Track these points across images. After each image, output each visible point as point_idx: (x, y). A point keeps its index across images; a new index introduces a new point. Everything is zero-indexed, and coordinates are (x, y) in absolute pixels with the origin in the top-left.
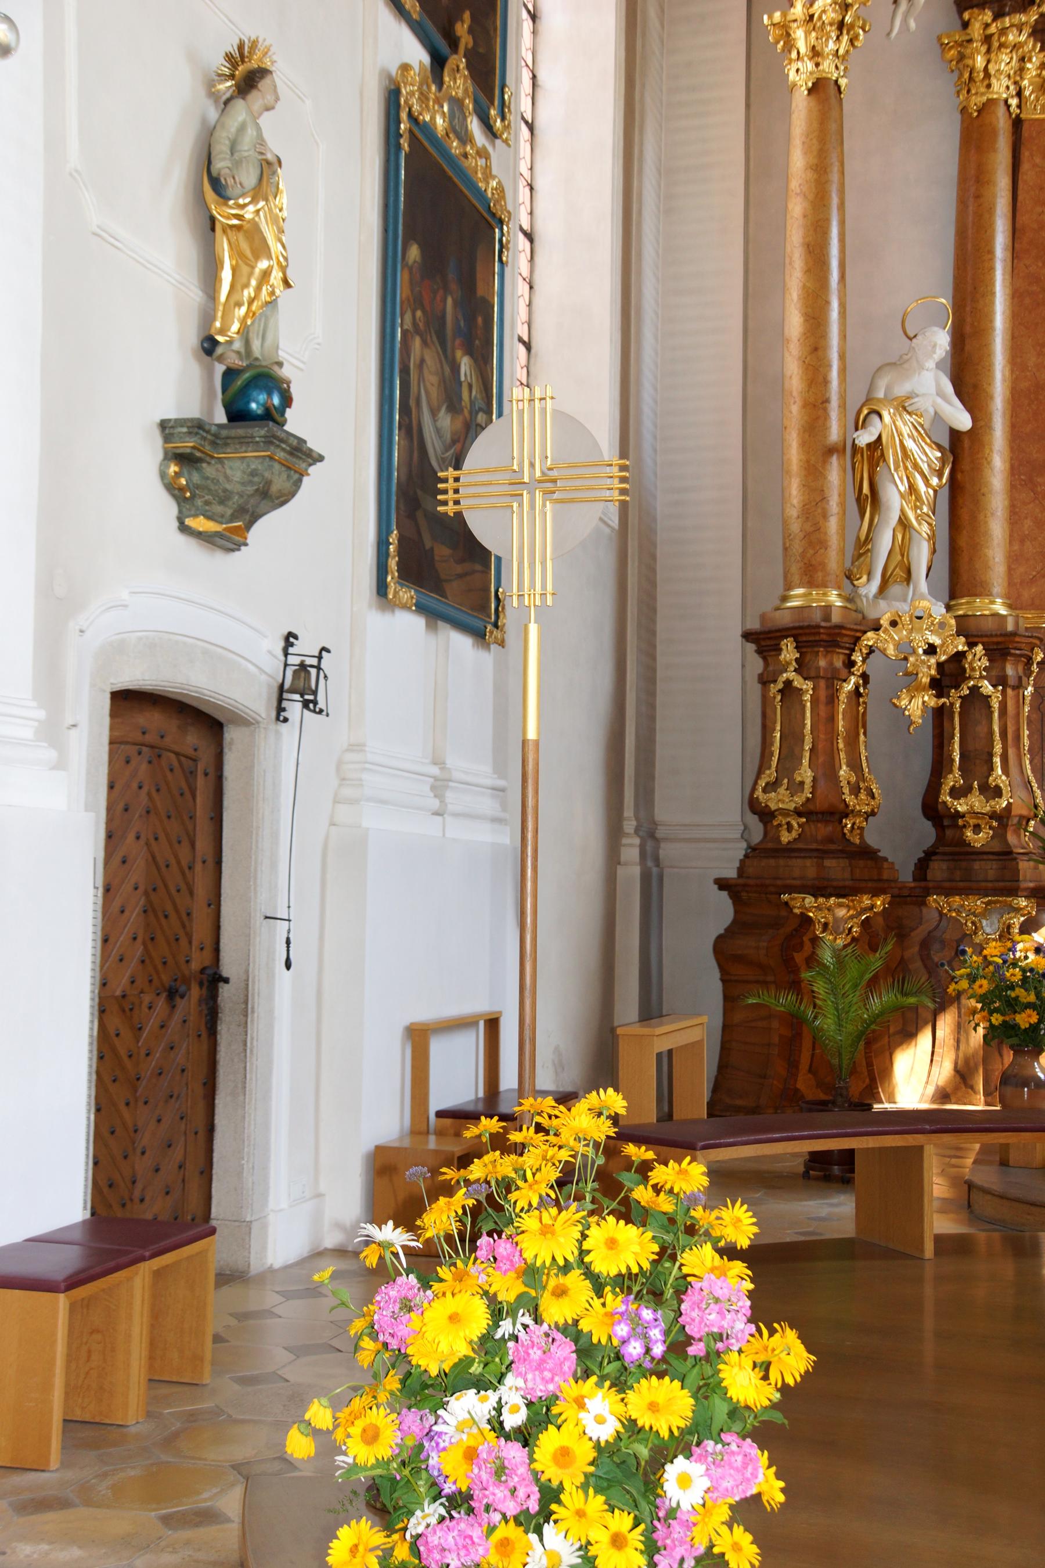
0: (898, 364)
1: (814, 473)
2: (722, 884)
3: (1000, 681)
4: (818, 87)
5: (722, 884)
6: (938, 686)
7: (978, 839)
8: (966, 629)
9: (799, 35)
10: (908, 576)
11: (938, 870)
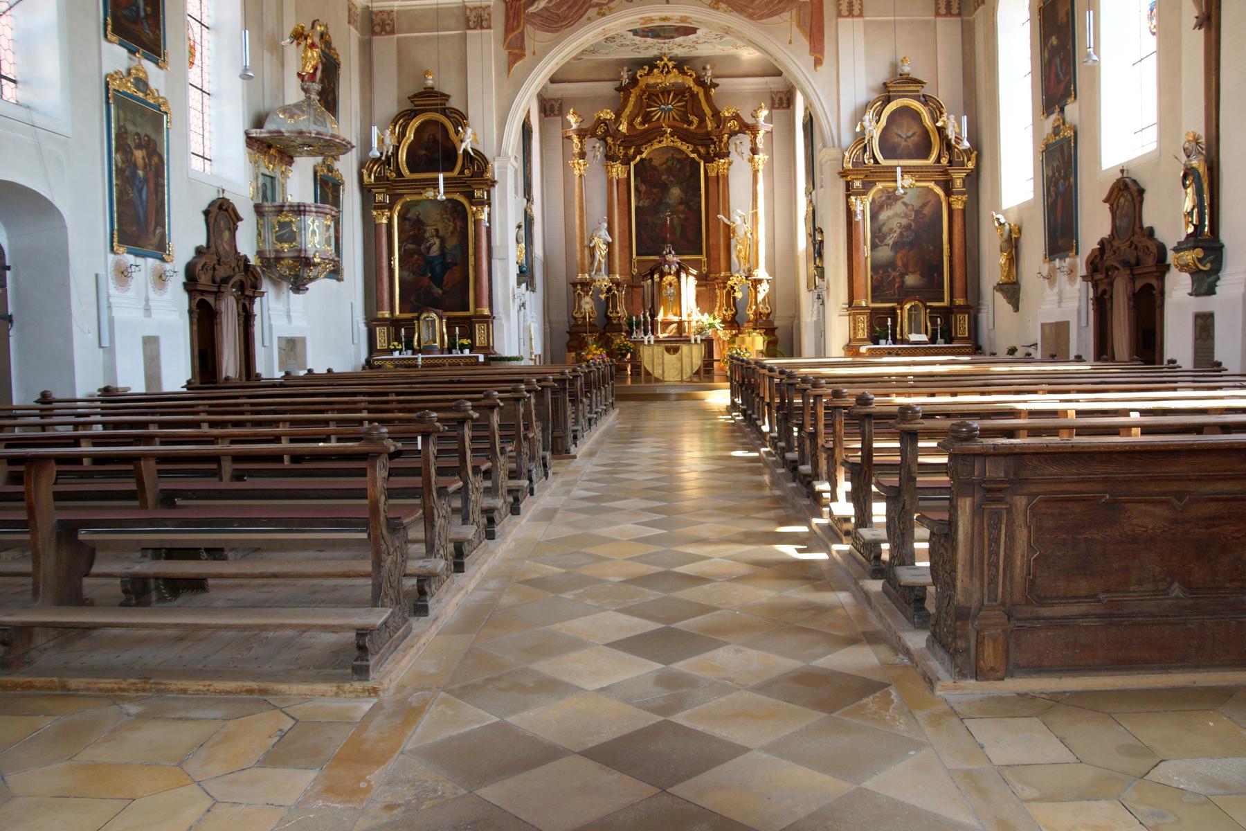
0: (598, 229)
1: (582, 251)
2: (568, 332)
3: (618, 291)
4: (581, 176)
5: (568, 332)
6: (607, 292)
7: (615, 322)
8: (612, 281)
9: (576, 166)
10: (601, 270)
11: (607, 328)
